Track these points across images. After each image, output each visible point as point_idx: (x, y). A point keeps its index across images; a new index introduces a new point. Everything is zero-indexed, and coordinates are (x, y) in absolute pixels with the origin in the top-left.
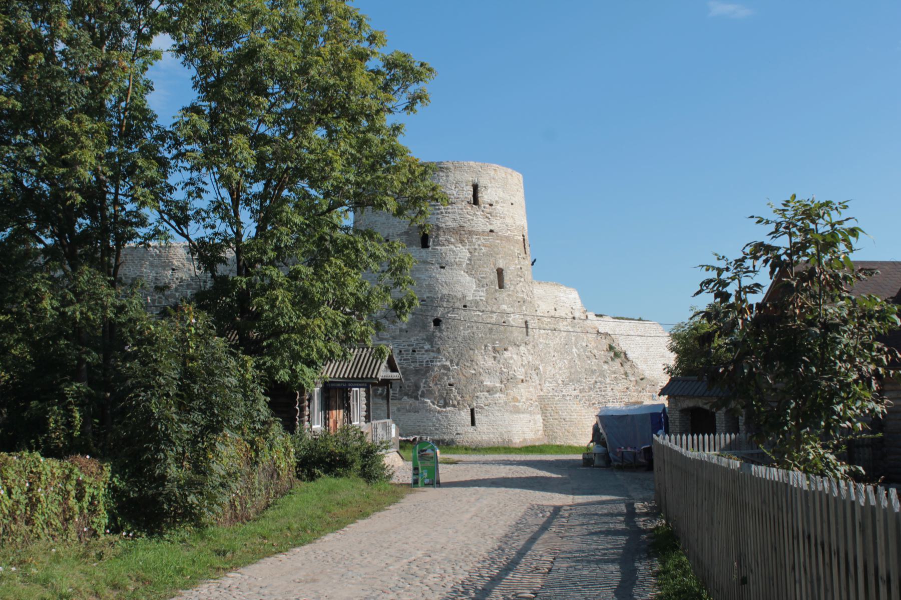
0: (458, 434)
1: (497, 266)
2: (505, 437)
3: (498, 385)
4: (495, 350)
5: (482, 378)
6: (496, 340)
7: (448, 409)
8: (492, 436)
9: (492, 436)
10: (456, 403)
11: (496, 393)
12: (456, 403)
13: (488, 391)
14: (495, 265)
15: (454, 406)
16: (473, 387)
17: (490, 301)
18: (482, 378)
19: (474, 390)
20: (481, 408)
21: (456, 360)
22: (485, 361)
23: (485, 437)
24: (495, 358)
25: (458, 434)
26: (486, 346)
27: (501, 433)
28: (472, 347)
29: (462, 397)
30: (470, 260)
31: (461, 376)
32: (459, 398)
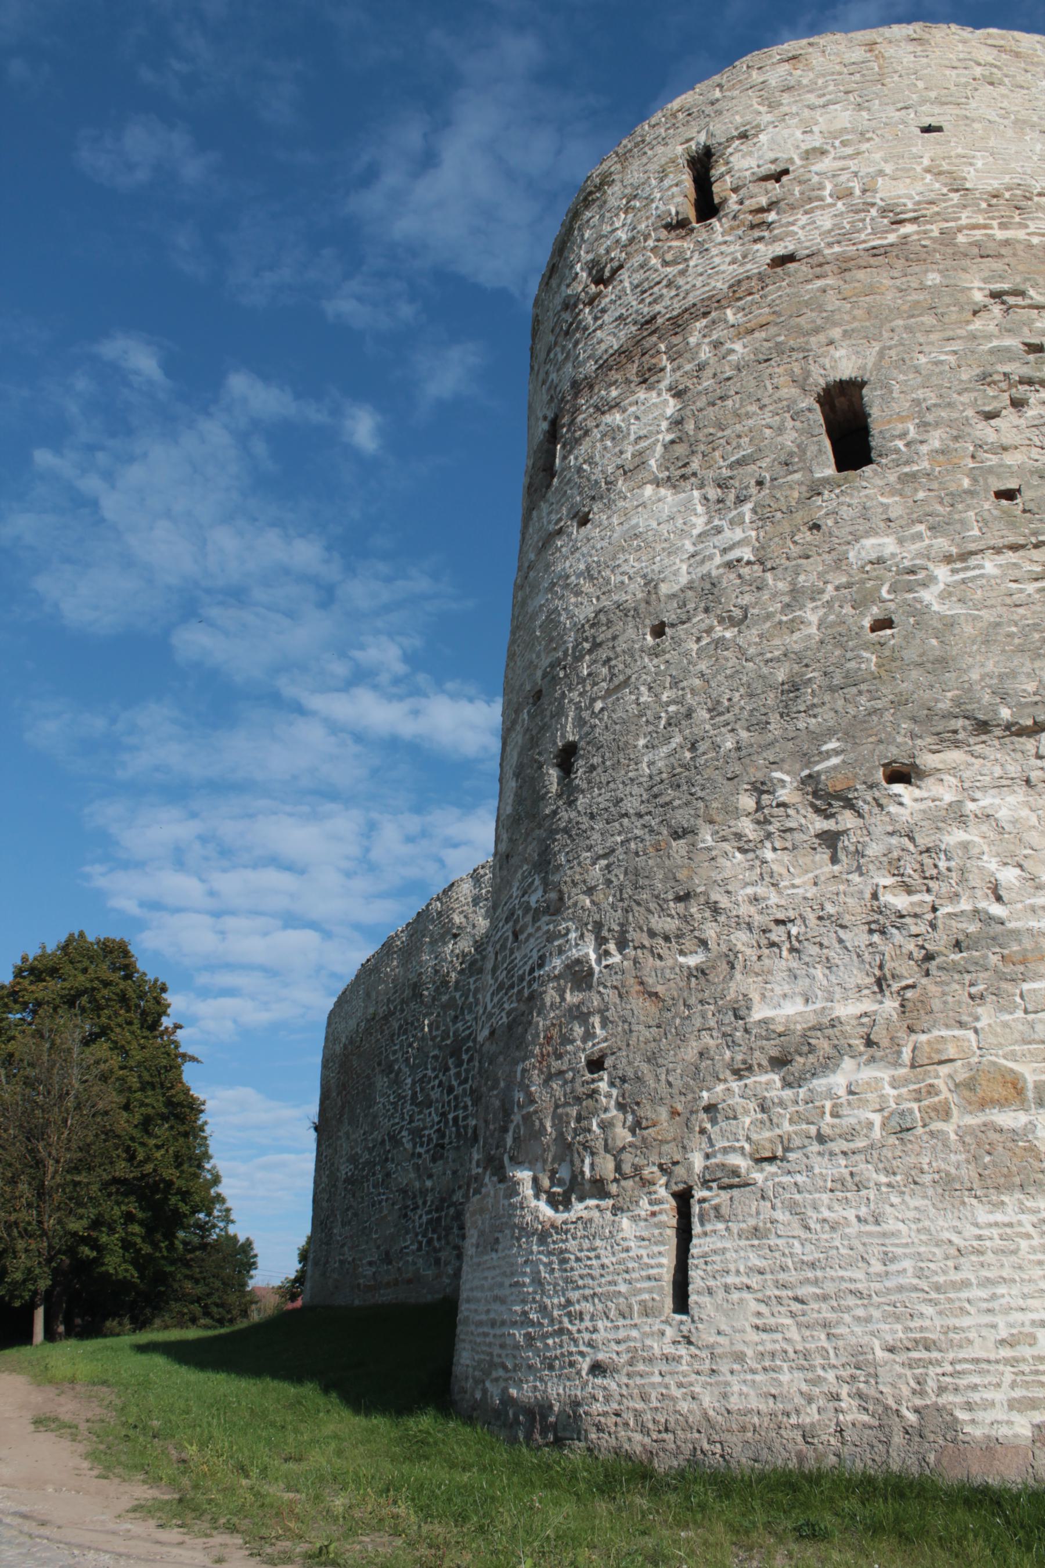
0: (597, 1369)
1: (819, 380)
2: (896, 1386)
3: (846, 1010)
4: (825, 798)
5: (742, 984)
6: (818, 737)
7: (579, 1208)
8: (791, 1380)
9: (791, 1380)
10: (607, 1166)
11: (829, 1064)
12: (607, 1166)
13: (779, 1062)
14: (801, 383)
15: (599, 1188)
16: (690, 1053)
17: (776, 552)
18: (742, 984)
19: (700, 1073)
20: (731, 1181)
21: (613, 920)
22: (759, 875)
23: (745, 1394)
24: (830, 840)
25: (597, 1369)
26: (760, 789)
27: (860, 1361)
28: (681, 817)
29: (636, 1126)
30: (678, 422)
31: (638, 1004)
32: (623, 1135)
